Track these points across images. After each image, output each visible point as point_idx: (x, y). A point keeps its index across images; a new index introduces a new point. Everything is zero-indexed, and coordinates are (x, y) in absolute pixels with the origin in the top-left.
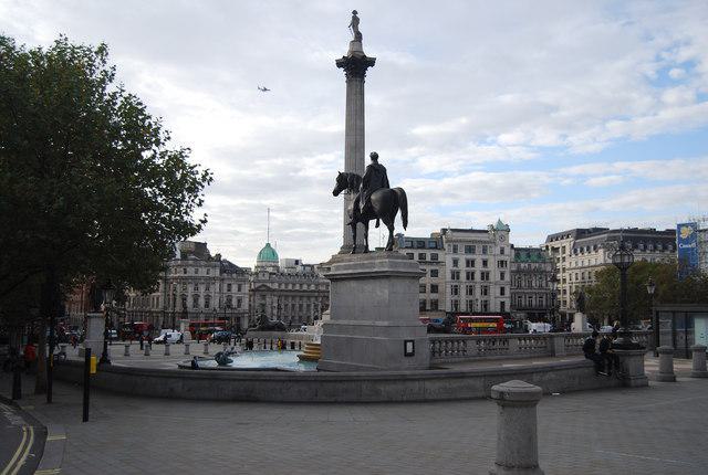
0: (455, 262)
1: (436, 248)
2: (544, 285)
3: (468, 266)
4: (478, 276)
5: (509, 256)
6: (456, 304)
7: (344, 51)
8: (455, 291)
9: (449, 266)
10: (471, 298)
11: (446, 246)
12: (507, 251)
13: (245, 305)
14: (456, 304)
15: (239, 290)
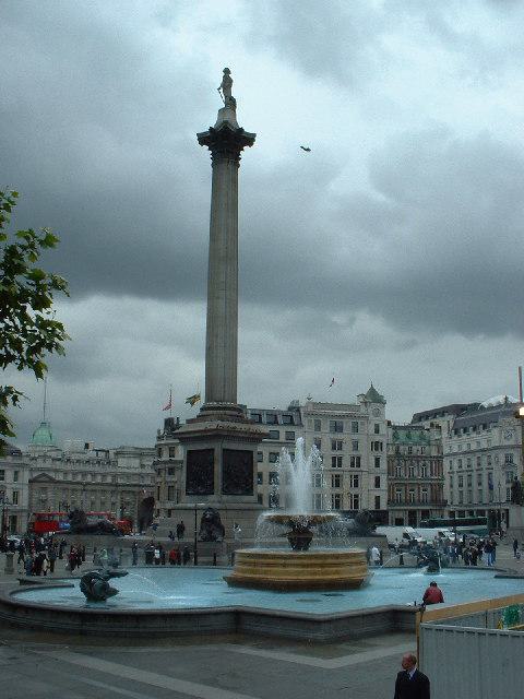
1: (292, 423)
2: (429, 474)
4: (346, 463)
5: (385, 435)
7: (210, 121)
10: (337, 491)
11: (305, 421)
12: (383, 429)
13: (24, 502)
15: (16, 479)
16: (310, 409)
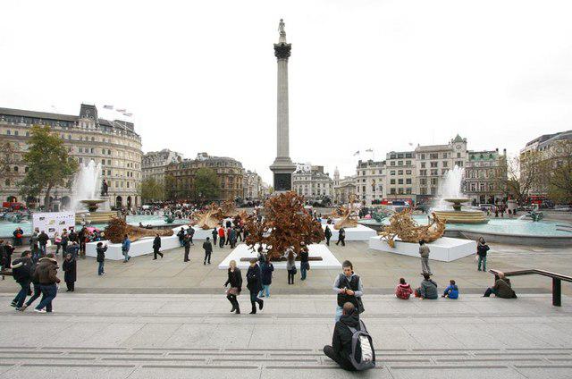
0: (423, 165)
3: (432, 166)
6: (424, 190)
8: (423, 182)
9: (419, 167)
12: (463, 155)
14: (424, 190)
16: (419, 150)
